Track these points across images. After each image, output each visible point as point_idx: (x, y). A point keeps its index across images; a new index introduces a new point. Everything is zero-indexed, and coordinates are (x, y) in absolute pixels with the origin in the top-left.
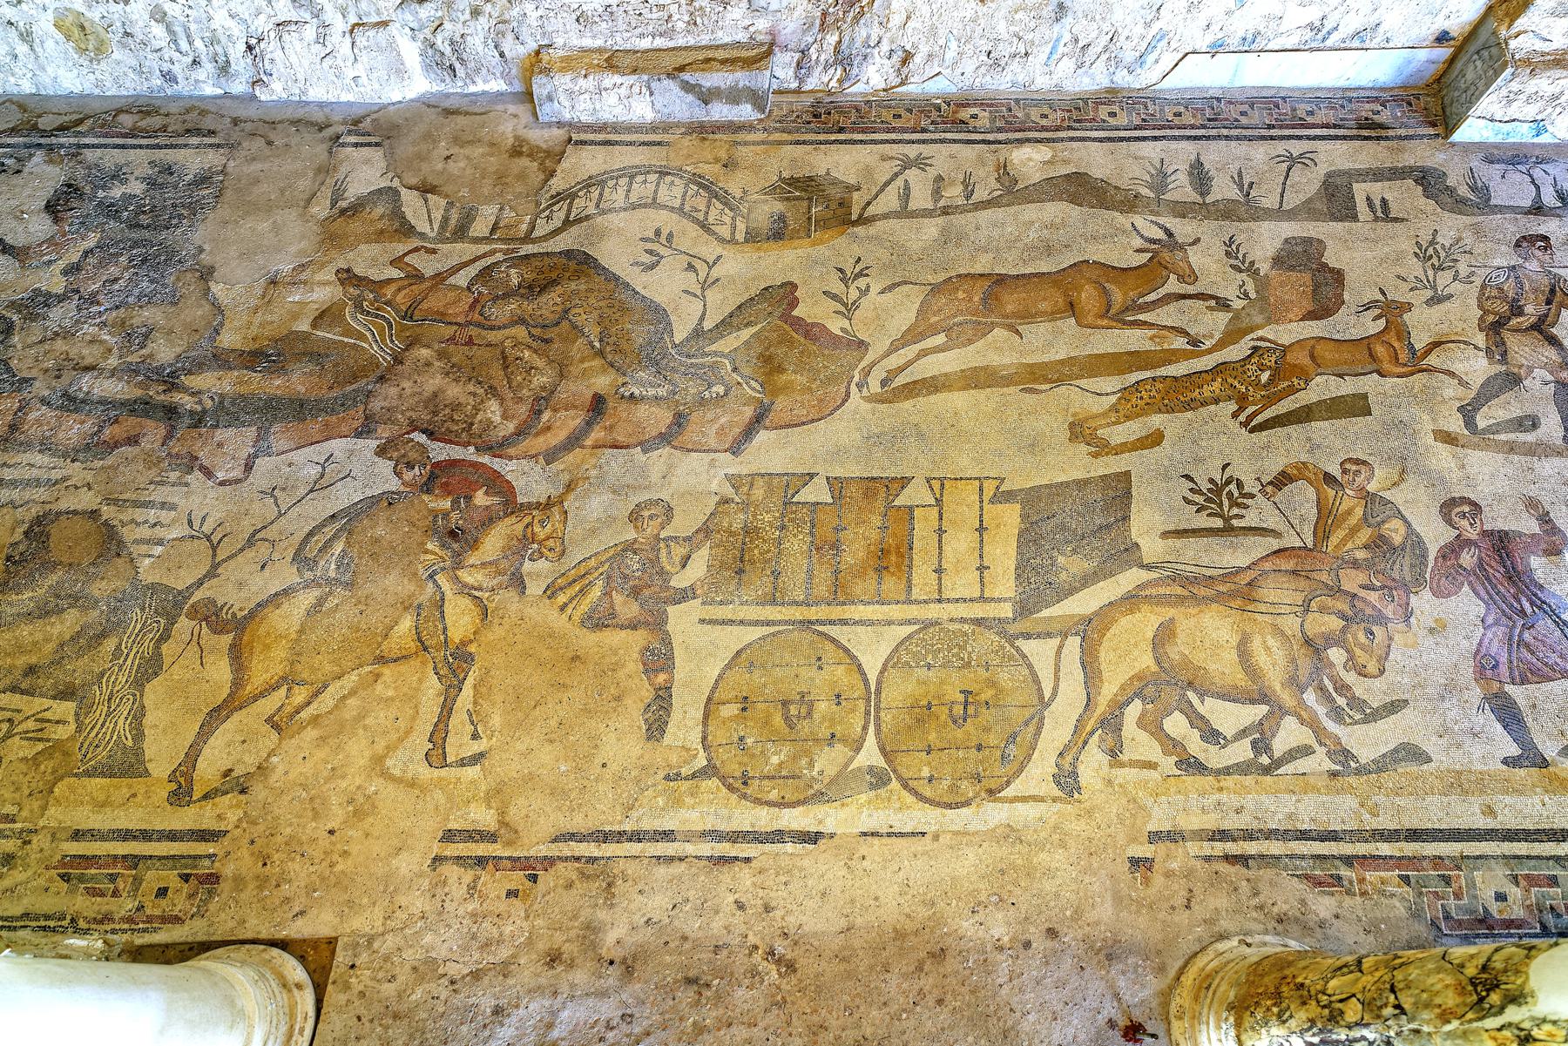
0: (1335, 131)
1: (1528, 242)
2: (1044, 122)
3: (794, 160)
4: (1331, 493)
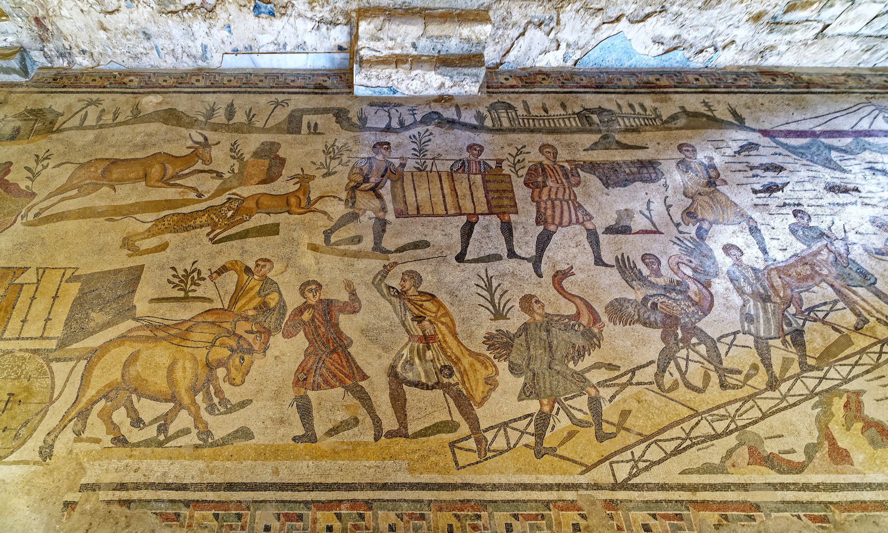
0: (303, 90)
1: (380, 146)
2: (164, 84)
3: (36, 101)
4: (246, 277)
